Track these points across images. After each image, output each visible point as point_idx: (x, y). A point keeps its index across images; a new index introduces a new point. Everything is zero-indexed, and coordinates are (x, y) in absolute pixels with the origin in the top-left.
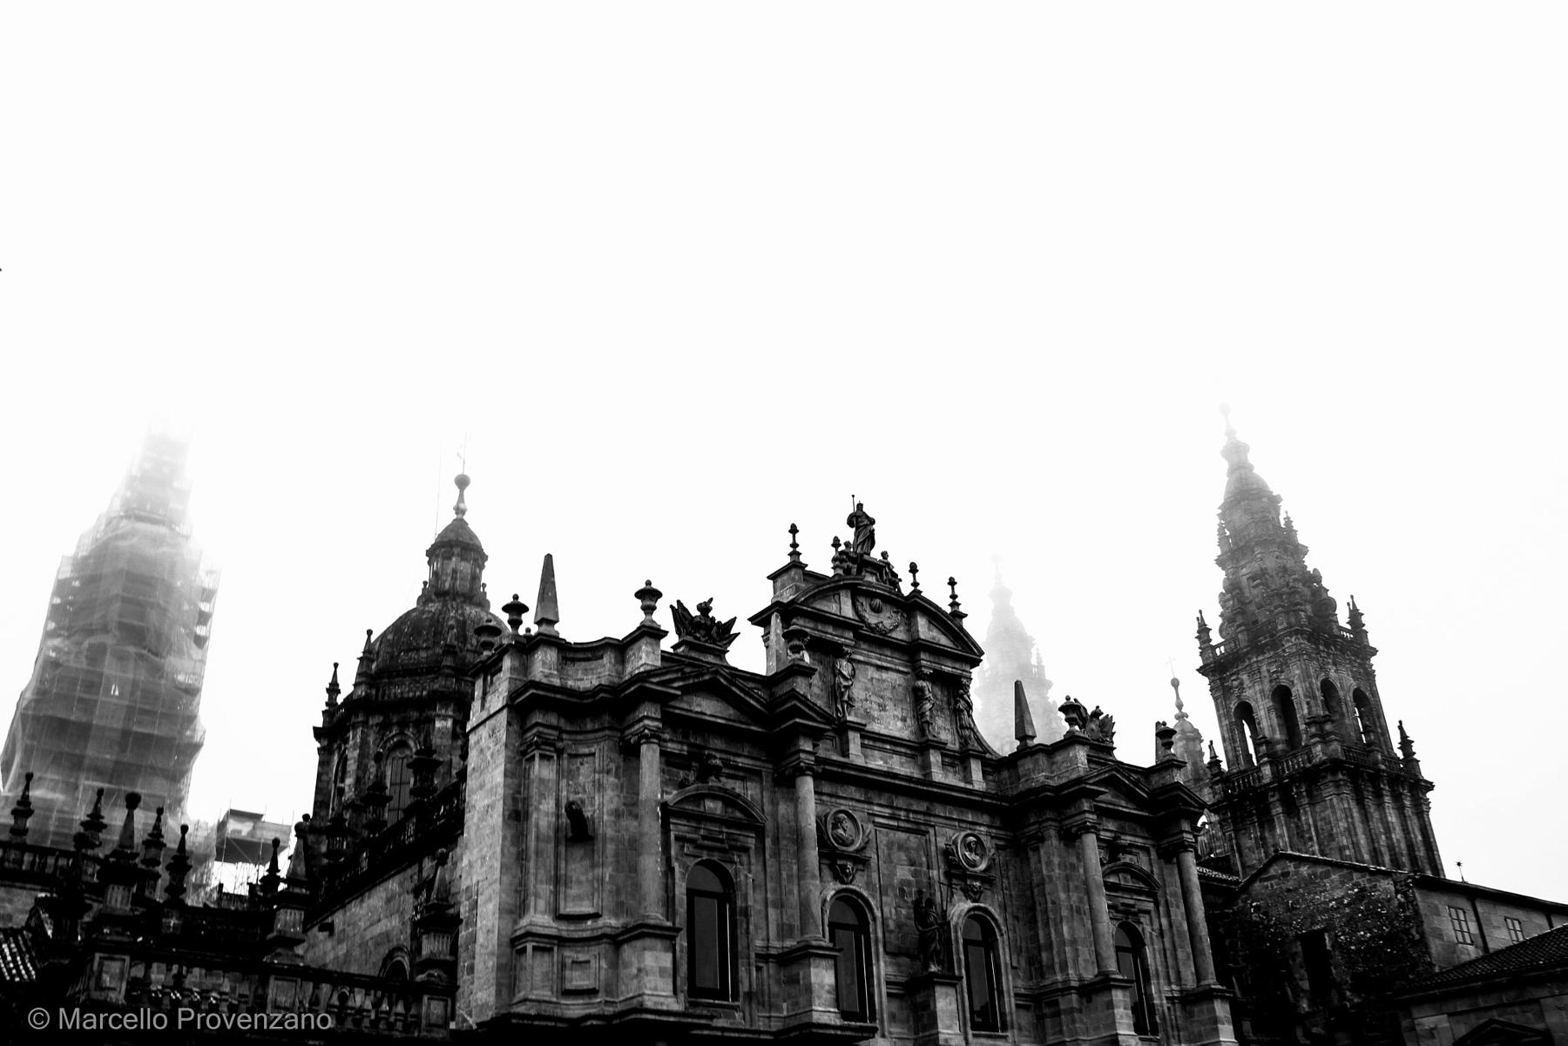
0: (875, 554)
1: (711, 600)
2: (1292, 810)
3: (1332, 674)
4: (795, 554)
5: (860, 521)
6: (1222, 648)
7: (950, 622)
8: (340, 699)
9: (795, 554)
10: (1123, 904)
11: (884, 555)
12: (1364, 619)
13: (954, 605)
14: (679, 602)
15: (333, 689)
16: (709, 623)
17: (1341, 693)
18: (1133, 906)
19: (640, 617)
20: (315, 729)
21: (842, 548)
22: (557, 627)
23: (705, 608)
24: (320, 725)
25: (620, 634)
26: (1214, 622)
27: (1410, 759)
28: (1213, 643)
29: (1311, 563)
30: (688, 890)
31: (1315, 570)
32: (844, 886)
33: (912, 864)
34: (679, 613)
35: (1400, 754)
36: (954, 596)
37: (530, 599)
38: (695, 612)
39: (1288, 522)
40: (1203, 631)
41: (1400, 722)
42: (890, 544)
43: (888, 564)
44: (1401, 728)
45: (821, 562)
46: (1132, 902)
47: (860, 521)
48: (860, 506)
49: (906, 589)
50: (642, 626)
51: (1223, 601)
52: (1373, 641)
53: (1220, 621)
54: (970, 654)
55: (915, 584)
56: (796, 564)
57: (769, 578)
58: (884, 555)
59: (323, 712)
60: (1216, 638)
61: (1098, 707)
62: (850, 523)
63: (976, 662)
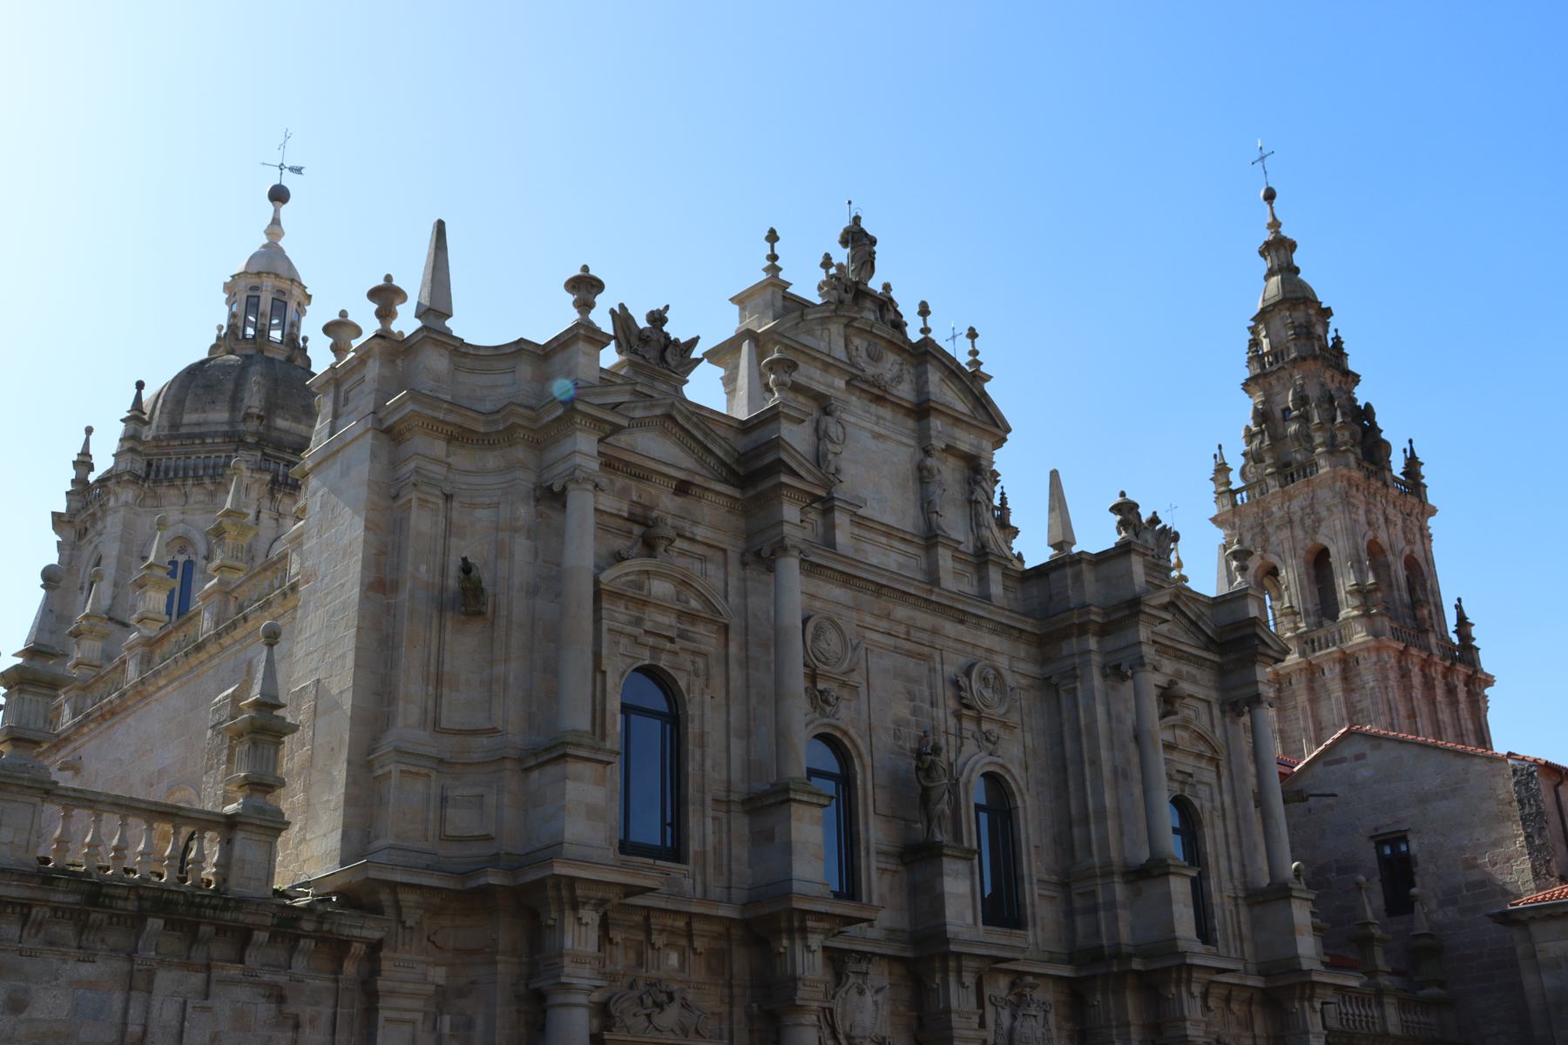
0: (875, 284)
1: (667, 307)
3: (1383, 537)
4: (773, 269)
5: (858, 239)
6: (1244, 494)
7: (971, 381)
8: (92, 477)
9: (773, 269)
10: (1179, 771)
11: (887, 287)
12: (1423, 470)
13: (976, 364)
14: (622, 306)
15: (84, 462)
16: (663, 340)
17: (1390, 558)
18: (1190, 775)
19: (573, 316)
21: (833, 271)
22: (448, 323)
23: (658, 318)
25: (542, 335)
26: (1236, 462)
27: (1466, 651)
28: (1233, 487)
29: (1362, 395)
30: (622, 704)
31: (1368, 406)
32: (826, 720)
33: (912, 700)
34: (622, 317)
35: (1455, 639)
36: (974, 353)
37: (413, 283)
38: (642, 323)
39: (1338, 342)
40: (1222, 469)
41: (1459, 600)
43: (891, 300)
44: (1459, 608)
45: (806, 284)
46: (1189, 770)
47: (858, 239)
48: (857, 219)
49: (914, 335)
50: (577, 325)
51: (1250, 436)
52: (1432, 498)
53: (1242, 461)
54: (996, 428)
55: (925, 330)
56: (774, 282)
57: (732, 300)
58: (887, 287)
59: (67, 493)
60: (1237, 483)
61: (1155, 513)
62: (844, 242)
63: (1000, 441)
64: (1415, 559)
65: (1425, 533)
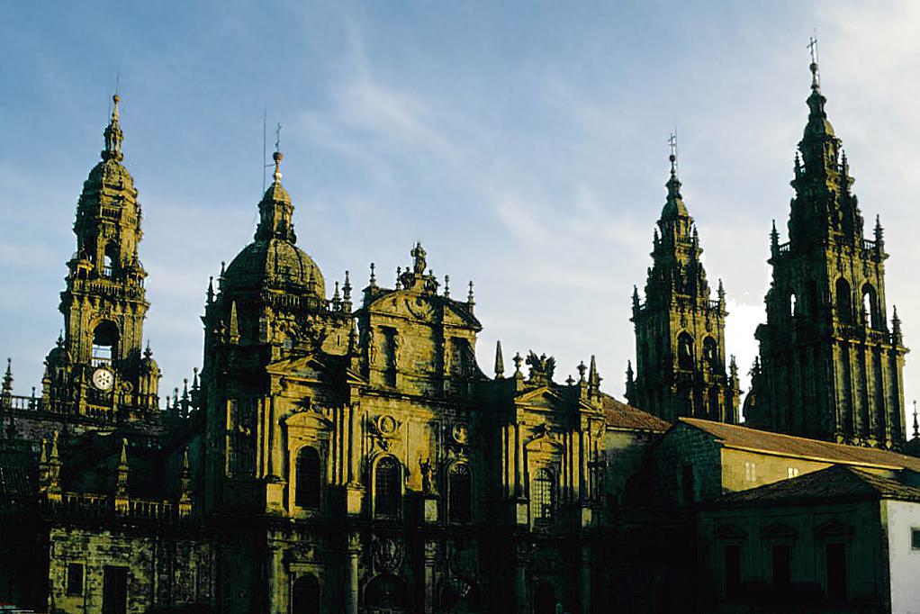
0: (426, 273)
2: (804, 360)
3: (847, 275)
4: (372, 281)
11: (431, 272)
13: (470, 298)
15: (210, 293)
20: (202, 317)
21: (403, 271)
24: (204, 315)
28: (780, 244)
31: (855, 196)
40: (775, 236)
42: (434, 266)
45: (388, 281)
47: (418, 253)
49: (440, 292)
58: (431, 272)
64: (871, 286)
65: (880, 269)
